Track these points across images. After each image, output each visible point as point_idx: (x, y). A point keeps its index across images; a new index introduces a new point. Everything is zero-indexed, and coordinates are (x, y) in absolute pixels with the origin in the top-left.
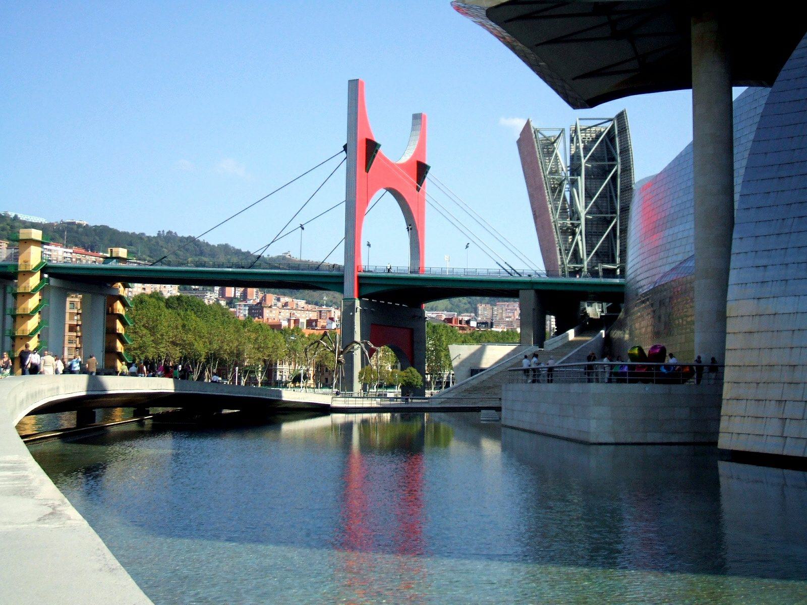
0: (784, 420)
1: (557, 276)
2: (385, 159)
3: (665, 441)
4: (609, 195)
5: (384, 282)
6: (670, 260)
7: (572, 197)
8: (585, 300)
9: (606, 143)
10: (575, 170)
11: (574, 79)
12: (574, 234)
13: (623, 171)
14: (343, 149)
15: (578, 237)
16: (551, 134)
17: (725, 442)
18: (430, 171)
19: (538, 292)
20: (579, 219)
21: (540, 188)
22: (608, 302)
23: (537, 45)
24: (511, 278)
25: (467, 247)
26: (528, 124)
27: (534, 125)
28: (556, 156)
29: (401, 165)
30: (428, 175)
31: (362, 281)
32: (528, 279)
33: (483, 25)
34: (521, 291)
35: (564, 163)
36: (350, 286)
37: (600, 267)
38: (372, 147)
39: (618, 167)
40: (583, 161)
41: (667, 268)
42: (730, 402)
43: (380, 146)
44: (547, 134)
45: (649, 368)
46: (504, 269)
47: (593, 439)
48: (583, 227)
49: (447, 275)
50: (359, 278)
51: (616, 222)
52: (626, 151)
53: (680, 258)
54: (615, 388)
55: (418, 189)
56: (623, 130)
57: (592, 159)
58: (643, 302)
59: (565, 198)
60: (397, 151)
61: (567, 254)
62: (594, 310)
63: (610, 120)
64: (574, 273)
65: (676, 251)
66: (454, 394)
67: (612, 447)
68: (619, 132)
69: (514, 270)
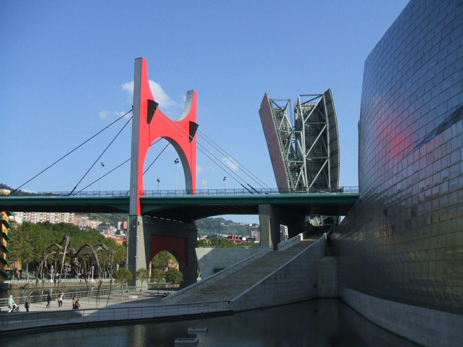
1: (287, 192)
2: (161, 113)
4: (321, 146)
5: (158, 202)
8: (308, 214)
9: (318, 112)
12: (299, 172)
13: (331, 128)
14: (132, 108)
15: (302, 172)
16: (282, 105)
18: (199, 128)
20: (302, 160)
21: (275, 139)
25: (224, 179)
29: (179, 123)
30: (197, 131)
32: (266, 195)
34: (260, 206)
35: (291, 124)
36: (134, 207)
39: (327, 126)
40: (304, 122)
43: (158, 104)
46: (246, 189)
50: (141, 199)
51: (327, 162)
52: (332, 115)
55: (191, 139)
59: (292, 147)
62: (315, 222)
63: (321, 96)
66: (189, 295)
68: (327, 104)
69: (254, 189)
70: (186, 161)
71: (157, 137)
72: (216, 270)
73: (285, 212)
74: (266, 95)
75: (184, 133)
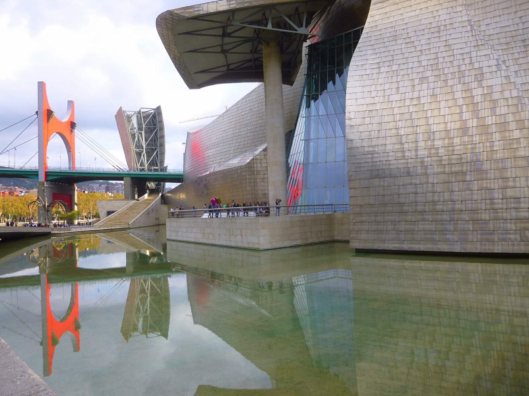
4: (155, 140)
5: (59, 174)
8: (147, 181)
10: (140, 129)
19: (132, 178)
20: (143, 148)
21: (127, 135)
24: (119, 173)
26: (121, 108)
27: (123, 109)
31: (47, 174)
36: (42, 177)
37: (153, 168)
38: (49, 113)
48: (145, 152)
49: (91, 171)
50: (46, 172)
60: (62, 115)
63: (154, 109)
64: (141, 170)
70: (70, 147)
71: (54, 132)
74: (121, 108)
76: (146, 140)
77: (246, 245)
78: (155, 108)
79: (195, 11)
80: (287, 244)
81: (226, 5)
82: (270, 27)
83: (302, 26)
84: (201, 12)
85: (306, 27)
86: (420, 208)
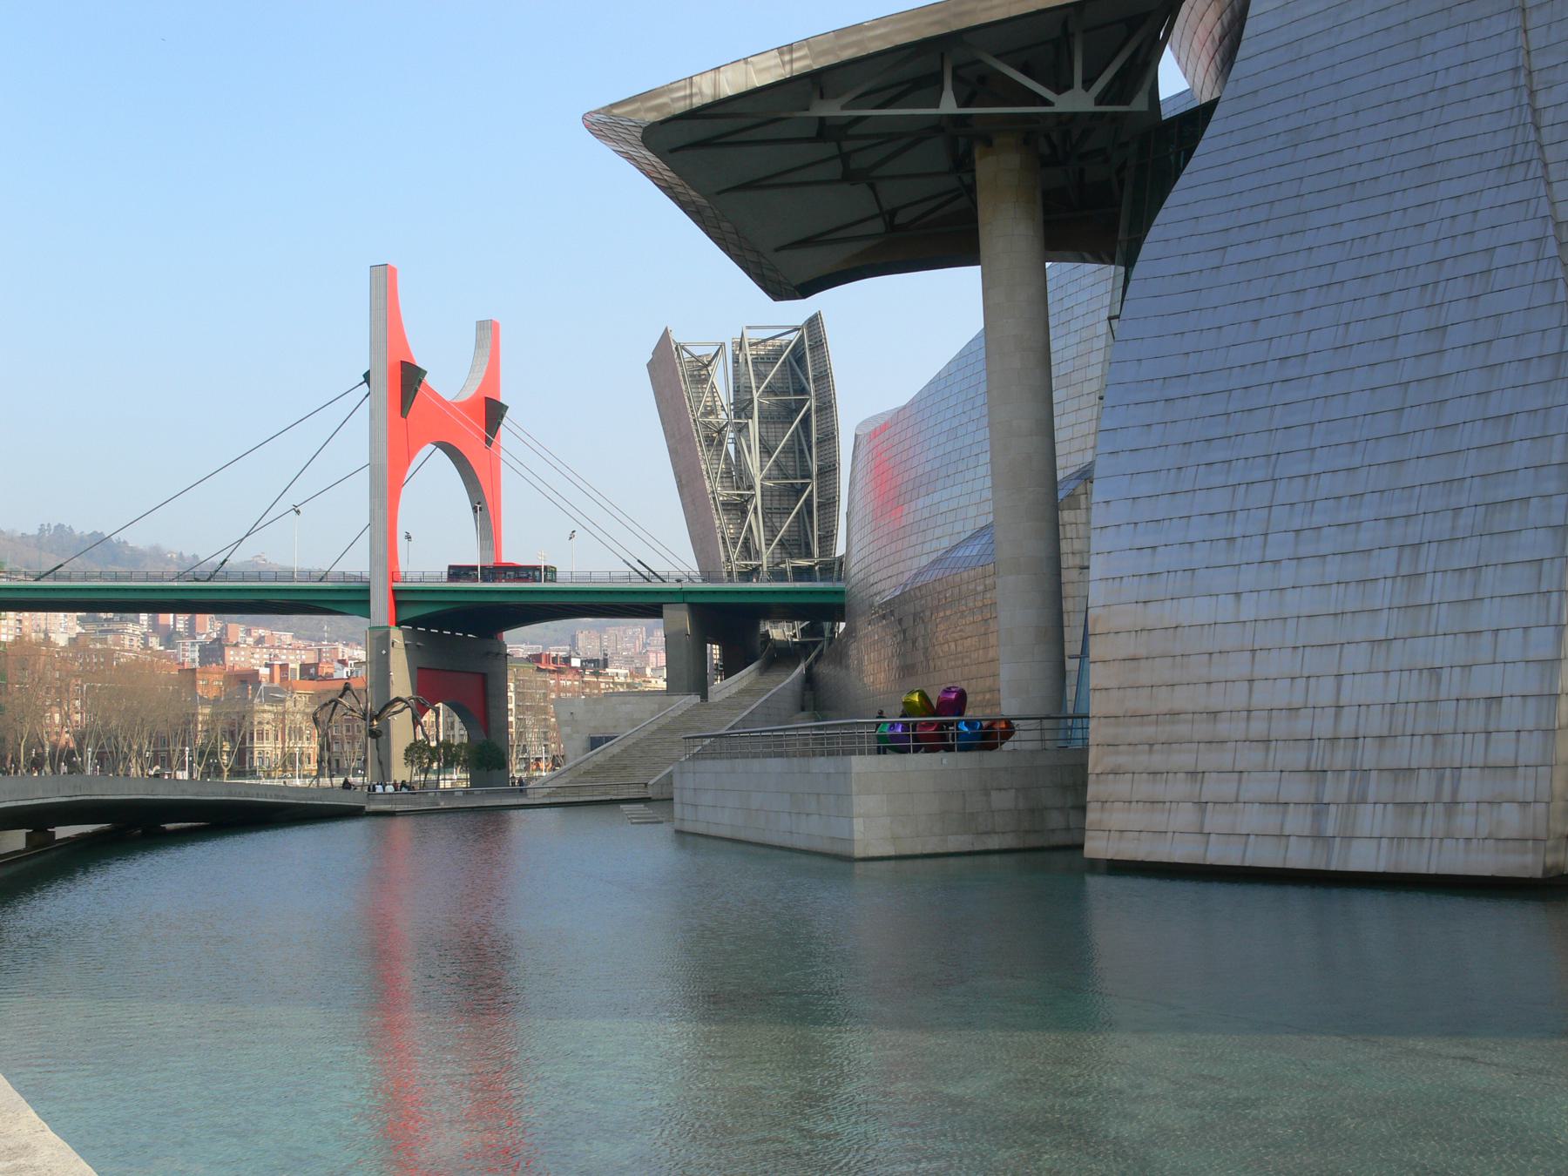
0: (1201, 805)
2: (435, 395)
3: (977, 848)
4: (799, 449)
6: (927, 548)
7: (737, 452)
10: (742, 408)
11: (777, 250)
12: (744, 513)
13: (819, 410)
15: (751, 516)
17: (1097, 846)
20: (751, 487)
21: (688, 438)
22: (802, 619)
23: (719, 193)
26: (666, 334)
27: (677, 337)
28: (713, 386)
29: (460, 405)
31: (399, 598)
32: (677, 586)
33: (630, 158)
38: (409, 378)
39: (812, 403)
40: (756, 395)
41: (925, 561)
42: (1102, 777)
44: (697, 351)
45: (941, 725)
47: (859, 852)
50: (395, 592)
52: (824, 377)
53: (946, 543)
54: (891, 761)
55: (488, 442)
56: (819, 344)
57: (770, 390)
58: (884, 617)
59: (727, 454)
60: (450, 379)
61: (735, 545)
62: (780, 632)
63: (797, 329)
64: (747, 575)
65: (938, 532)
67: (893, 863)
68: (812, 348)
72: (595, 742)
73: (721, 625)
74: (666, 334)
75: (473, 428)
76: (766, 450)
77: (801, 843)
78: (800, 323)
79: (673, 100)
80: (955, 843)
81: (776, 66)
82: (948, 105)
83: (1069, 87)
84: (697, 102)
85: (1088, 83)
86: (1258, 728)
